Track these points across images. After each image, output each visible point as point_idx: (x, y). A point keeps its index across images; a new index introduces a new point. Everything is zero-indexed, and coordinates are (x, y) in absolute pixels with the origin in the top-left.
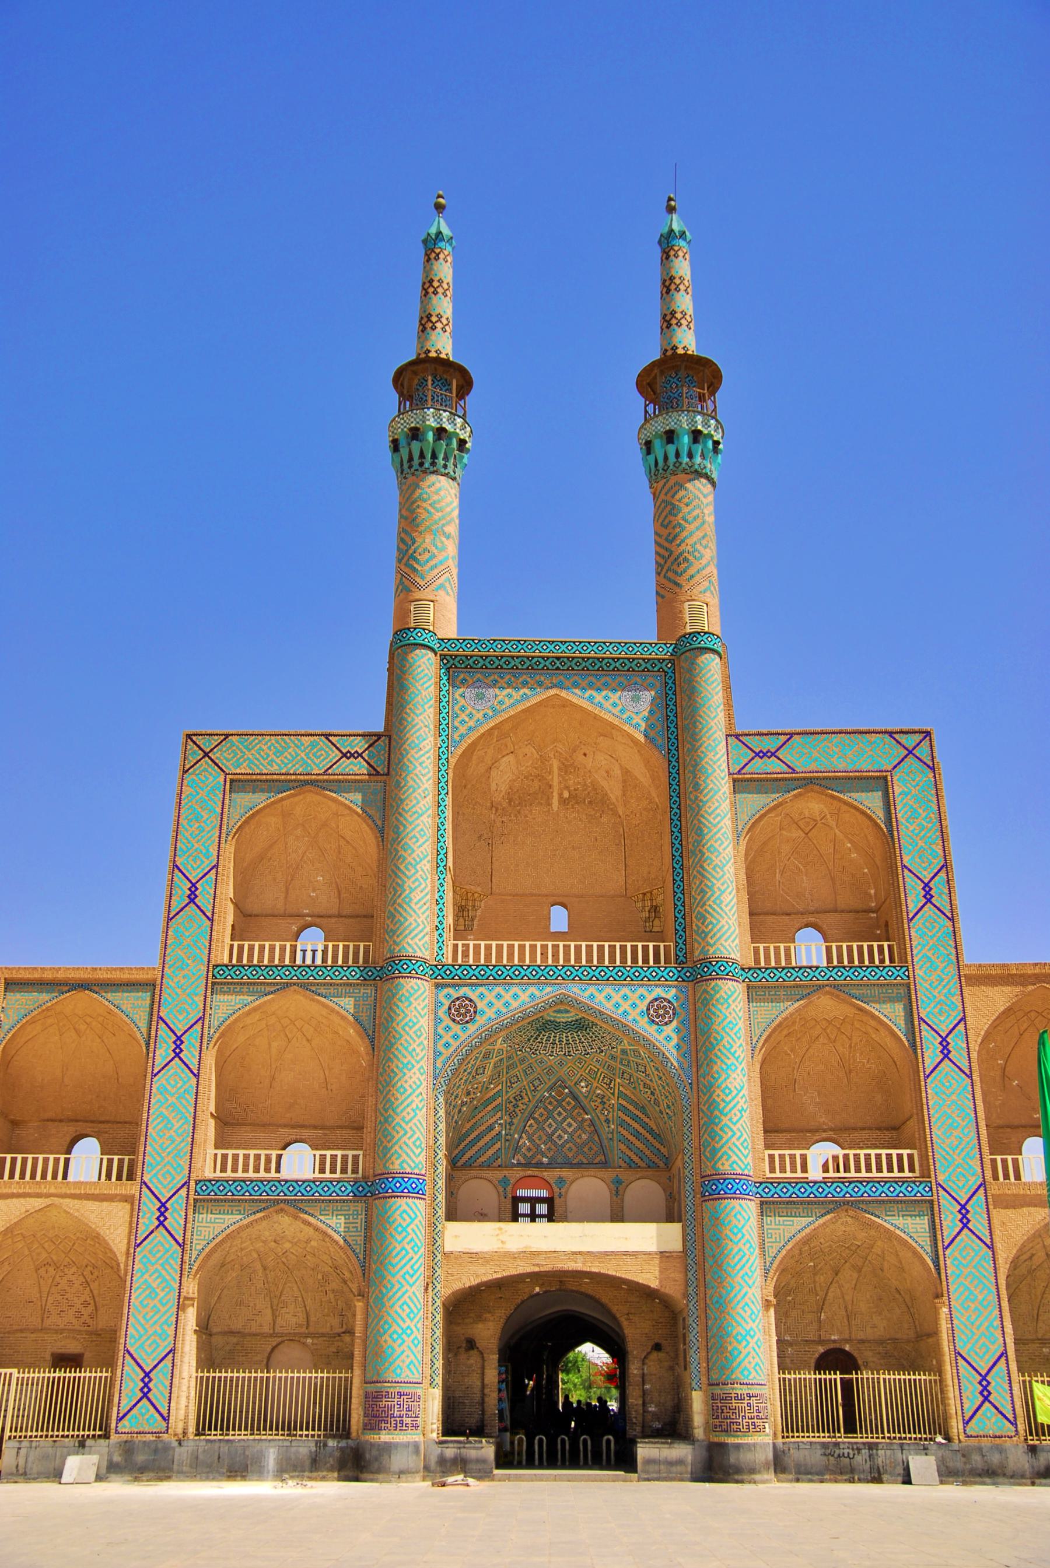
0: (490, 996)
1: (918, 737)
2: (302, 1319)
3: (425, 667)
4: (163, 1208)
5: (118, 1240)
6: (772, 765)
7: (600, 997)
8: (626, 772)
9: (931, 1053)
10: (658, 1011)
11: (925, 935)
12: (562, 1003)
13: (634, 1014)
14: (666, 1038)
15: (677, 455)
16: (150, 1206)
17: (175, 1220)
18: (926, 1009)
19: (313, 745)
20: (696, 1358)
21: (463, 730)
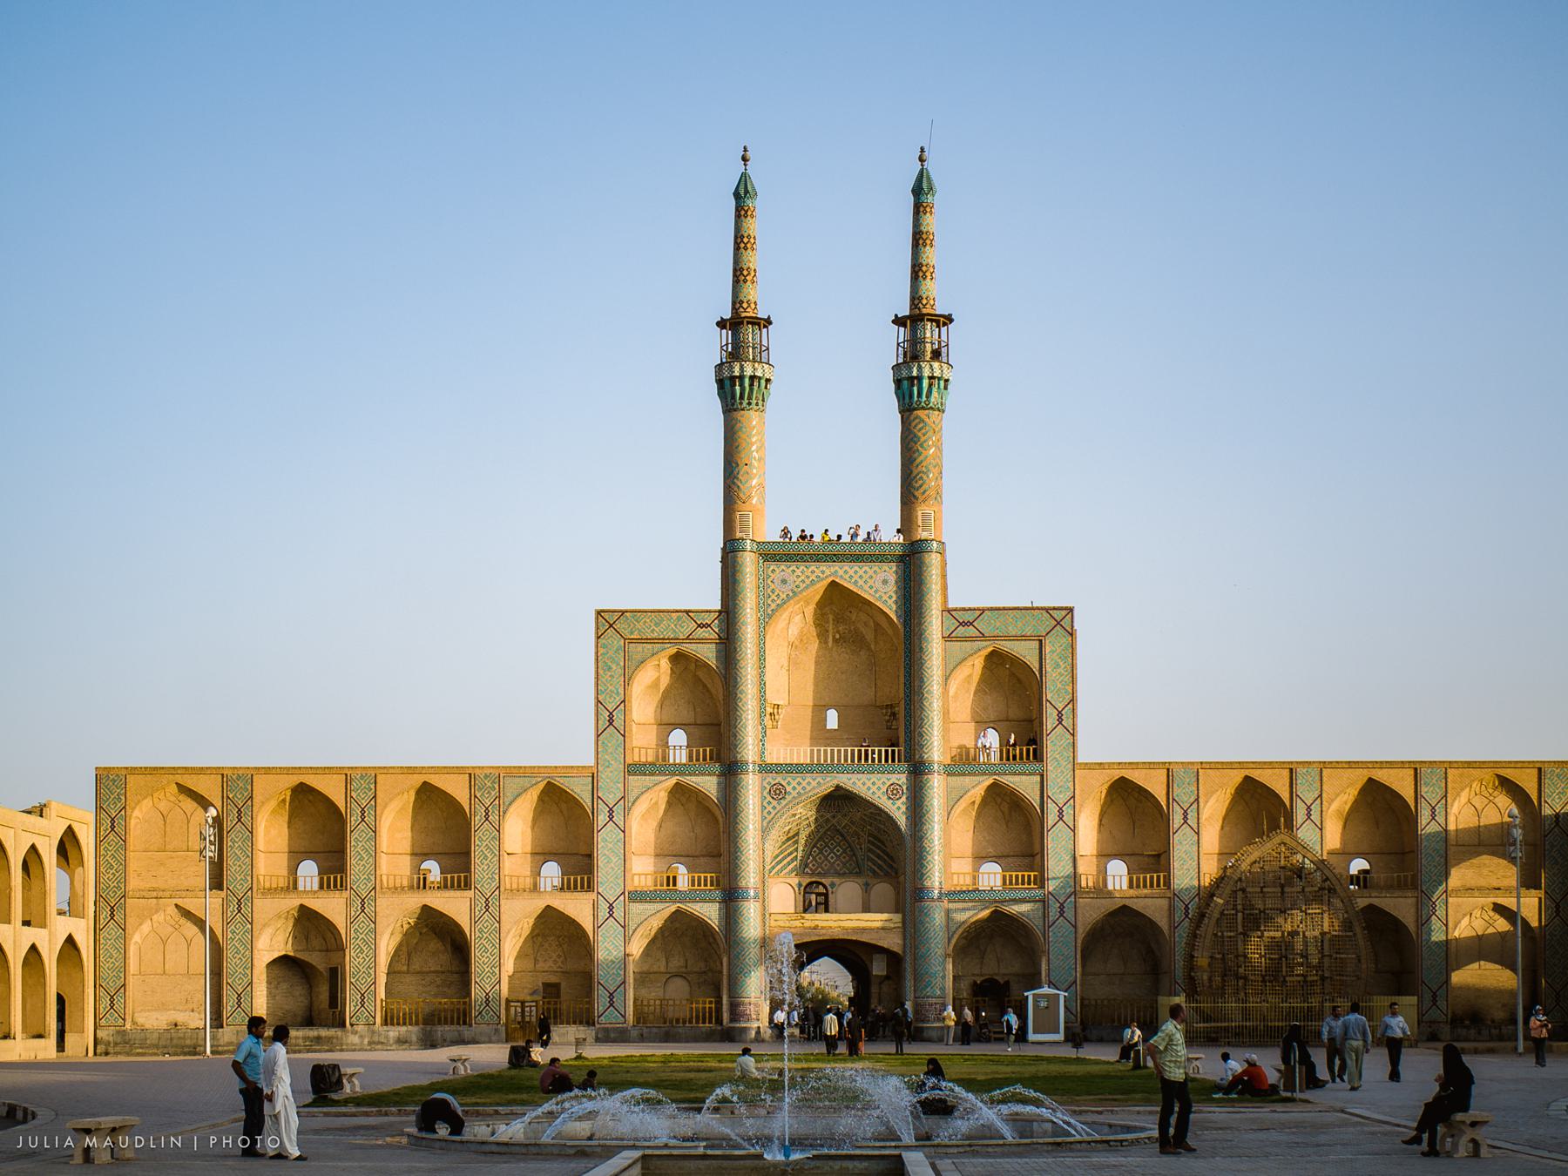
0: (794, 783)
1: (1064, 613)
2: (682, 963)
3: (749, 562)
4: (611, 907)
5: (588, 925)
6: (971, 631)
7: (859, 784)
8: (877, 625)
9: (1051, 817)
10: (892, 792)
11: (1054, 745)
12: (838, 788)
13: (879, 793)
14: (898, 811)
15: (920, 395)
16: (604, 906)
17: (618, 913)
18: (1051, 791)
19: (679, 619)
20: (909, 984)
21: (773, 606)
